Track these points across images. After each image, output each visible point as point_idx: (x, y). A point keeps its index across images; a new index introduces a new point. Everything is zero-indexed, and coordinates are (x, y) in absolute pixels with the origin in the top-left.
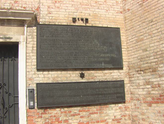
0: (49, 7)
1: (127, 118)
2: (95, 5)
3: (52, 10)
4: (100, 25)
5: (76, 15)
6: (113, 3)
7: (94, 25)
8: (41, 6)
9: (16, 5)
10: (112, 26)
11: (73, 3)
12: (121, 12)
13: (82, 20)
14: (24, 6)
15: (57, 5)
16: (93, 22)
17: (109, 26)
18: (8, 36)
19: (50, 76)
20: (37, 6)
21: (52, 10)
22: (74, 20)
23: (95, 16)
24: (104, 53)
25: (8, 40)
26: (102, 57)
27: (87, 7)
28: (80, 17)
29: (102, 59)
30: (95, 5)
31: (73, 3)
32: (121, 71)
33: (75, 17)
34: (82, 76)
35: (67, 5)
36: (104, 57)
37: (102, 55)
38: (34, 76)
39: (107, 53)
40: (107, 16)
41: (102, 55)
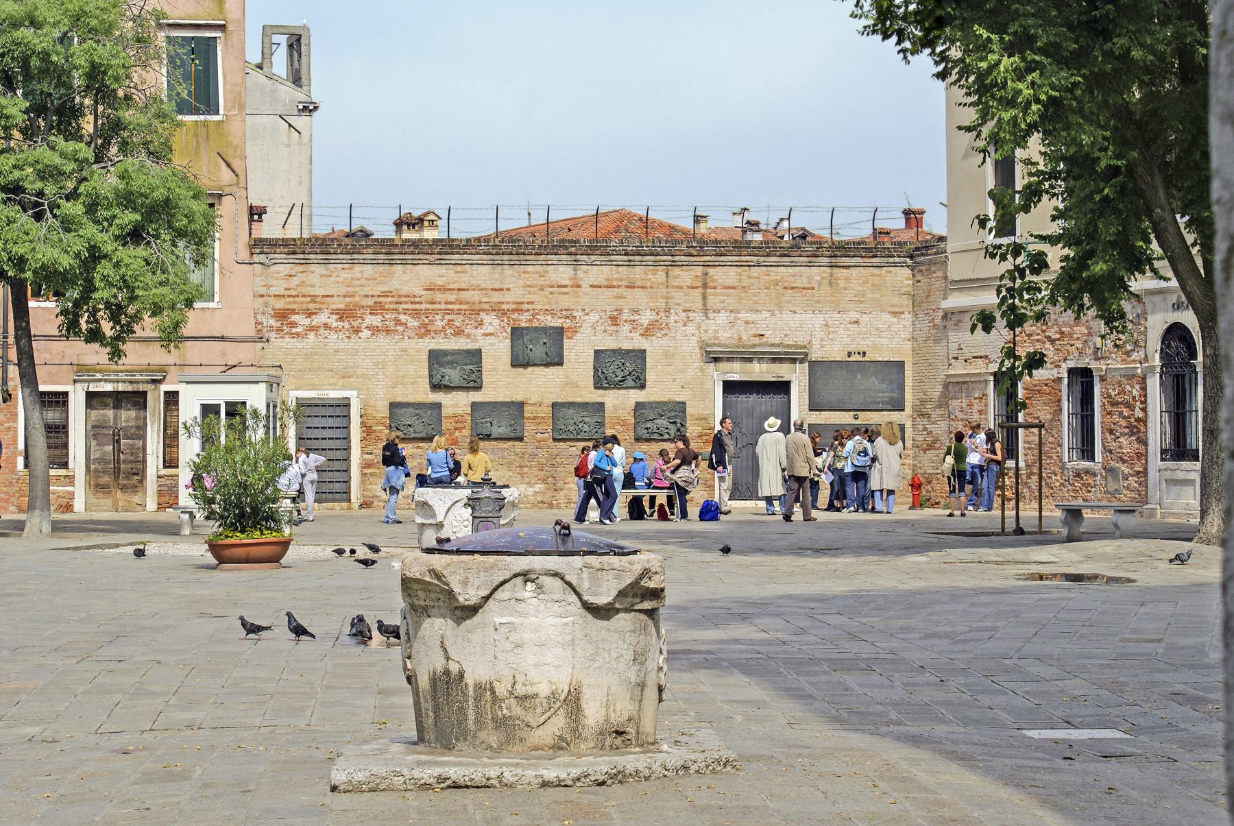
0: (821, 340)
1: (906, 467)
2: (875, 333)
3: (825, 343)
4: (881, 359)
5: (853, 348)
6: (899, 328)
7: (873, 359)
8: (813, 339)
9: (786, 339)
10: (896, 360)
11: (848, 333)
12: (909, 340)
13: (859, 353)
14: (795, 339)
15: (831, 336)
16: (871, 356)
17: (891, 360)
18: (780, 375)
19: (822, 416)
20: (808, 339)
21: (825, 343)
22: (850, 354)
23: (875, 347)
24: (882, 392)
25: (780, 379)
26: (879, 397)
27: (865, 336)
28: (857, 350)
29: (878, 400)
30: (875, 333)
31: (848, 333)
32: (902, 413)
33: (850, 350)
34: (856, 418)
35: (843, 336)
36: (882, 397)
37: (881, 395)
38: (806, 416)
39: (886, 392)
40: (890, 346)
41: (881, 395)
